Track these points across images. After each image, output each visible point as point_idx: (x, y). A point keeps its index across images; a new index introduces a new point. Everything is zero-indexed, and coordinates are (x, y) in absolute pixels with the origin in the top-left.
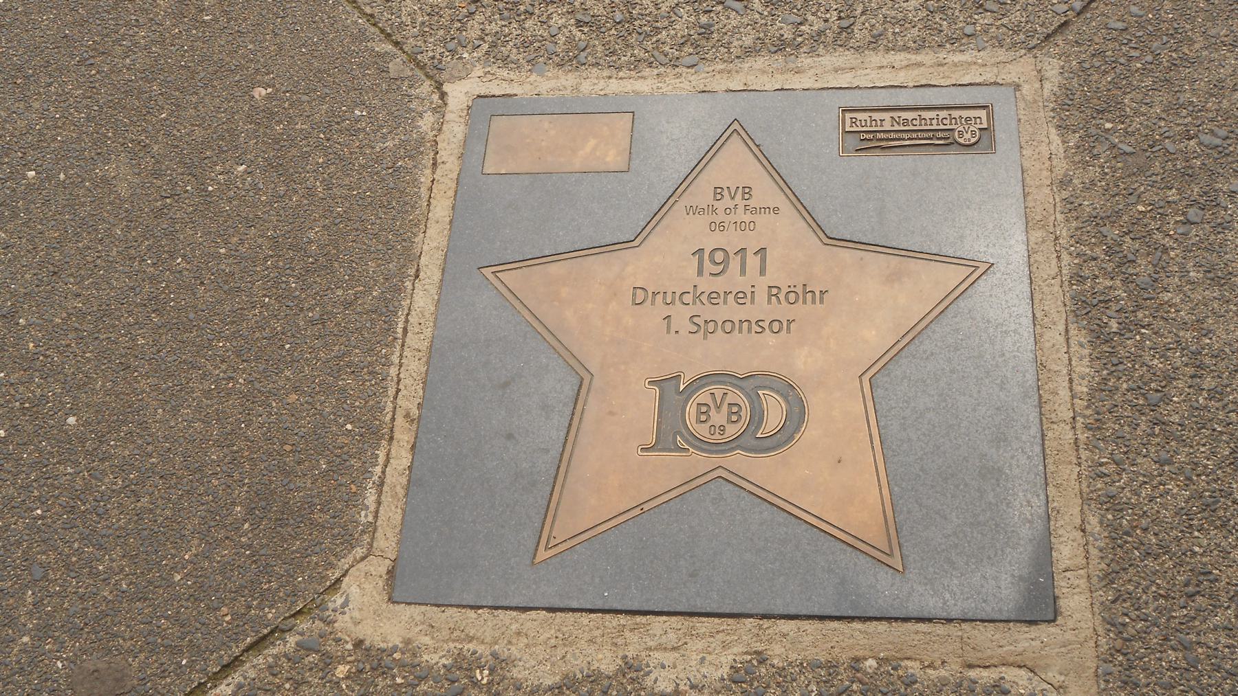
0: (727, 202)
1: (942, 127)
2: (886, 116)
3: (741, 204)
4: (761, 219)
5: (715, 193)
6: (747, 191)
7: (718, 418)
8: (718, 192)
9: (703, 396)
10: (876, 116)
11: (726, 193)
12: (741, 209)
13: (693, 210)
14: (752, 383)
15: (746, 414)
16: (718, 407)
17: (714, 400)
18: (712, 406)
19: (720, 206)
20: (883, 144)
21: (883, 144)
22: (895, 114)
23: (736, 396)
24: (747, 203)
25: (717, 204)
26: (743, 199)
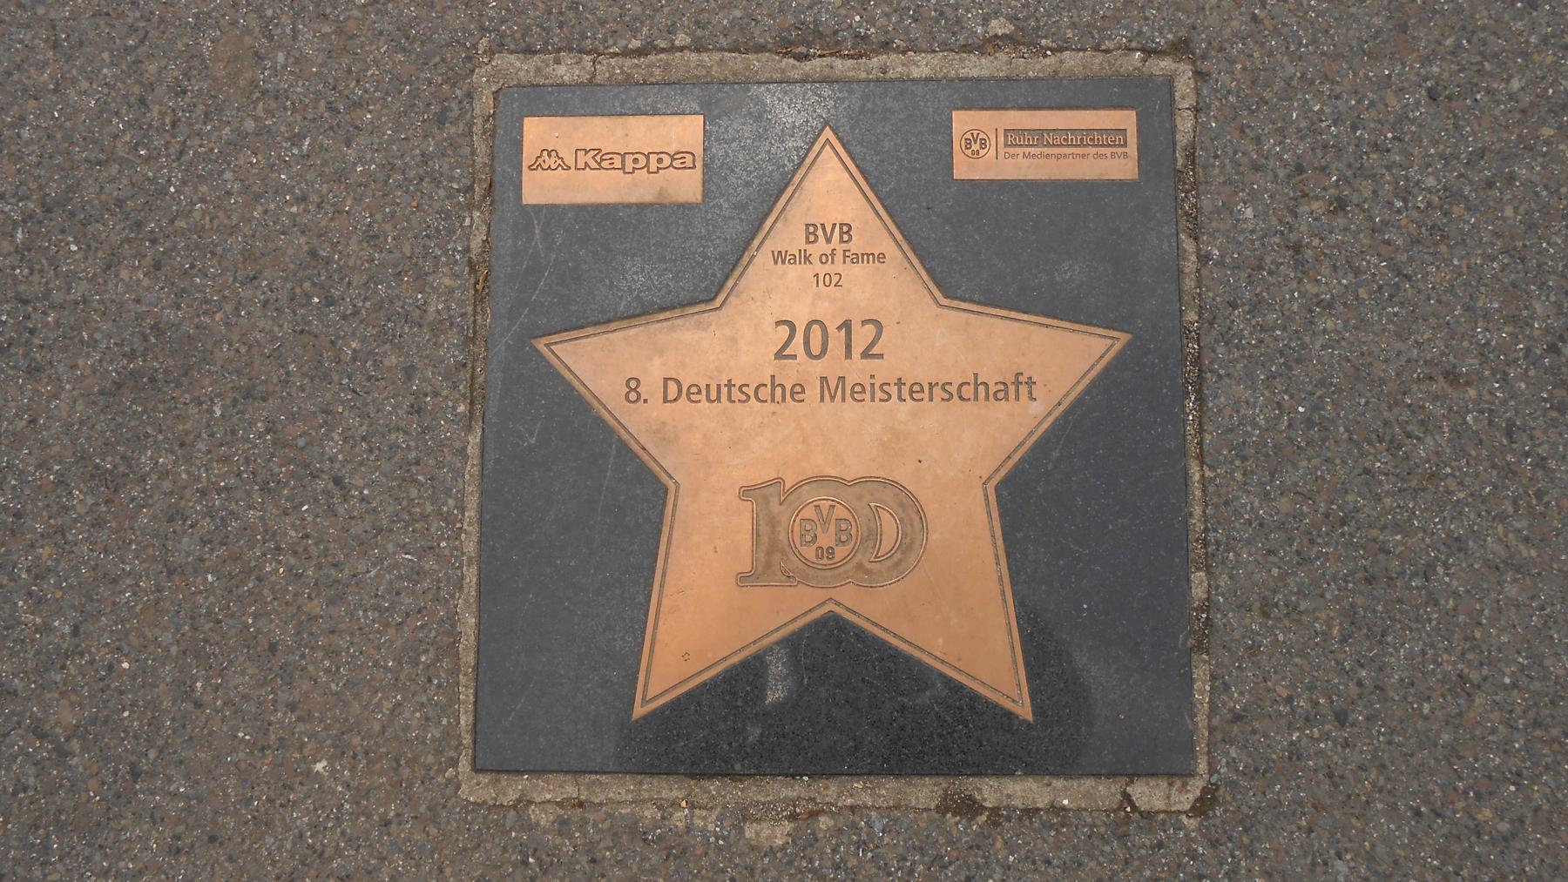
0: (821, 246)
3: (840, 248)
5: (808, 233)
8: (811, 232)
11: (820, 232)
13: (779, 258)
24: (845, 246)
25: (810, 248)
26: (842, 241)
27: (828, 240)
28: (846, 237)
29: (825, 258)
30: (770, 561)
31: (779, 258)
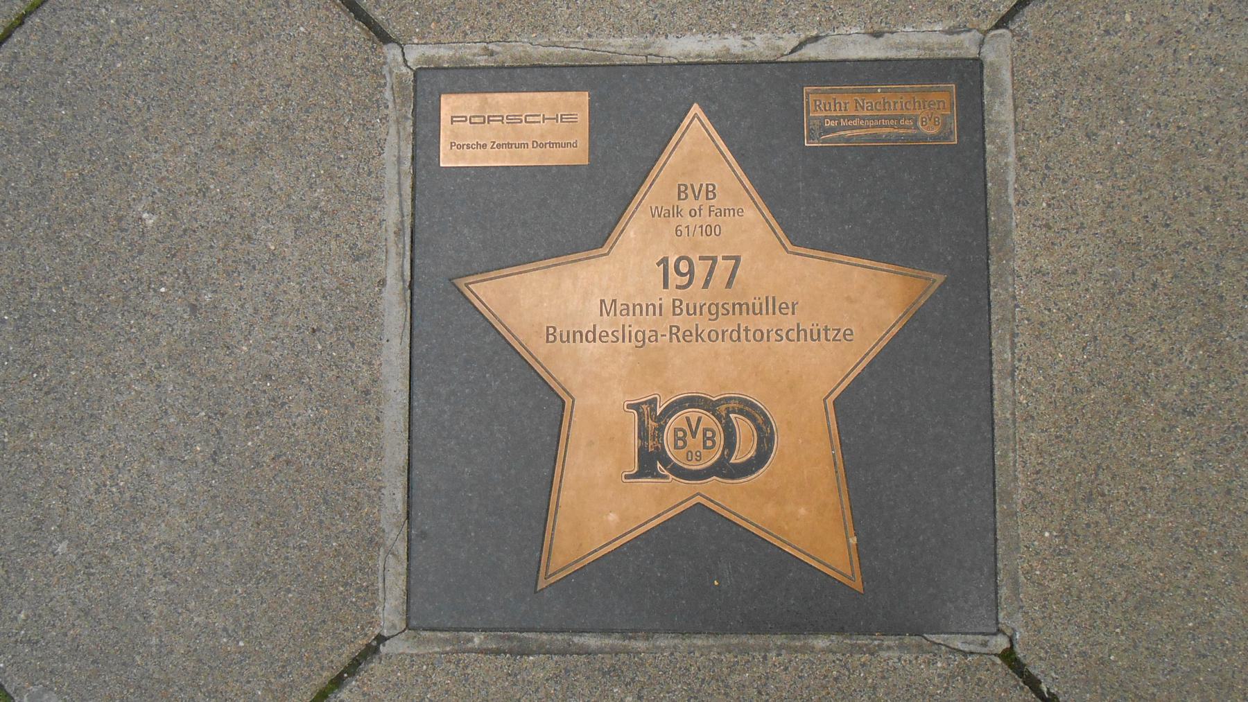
4: (727, 223)
6: (710, 192)
8: (682, 192)
11: (689, 191)
12: (705, 212)
13: (656, 213)
15: (720, 440)
16: (694, 437)
17: (690, 426)
19: (685, 206)
20: (848, 133)
21: (848, 133)
23: (709, 420)
27: (696, 198)
29: (693, 213)
30: (650, 462)
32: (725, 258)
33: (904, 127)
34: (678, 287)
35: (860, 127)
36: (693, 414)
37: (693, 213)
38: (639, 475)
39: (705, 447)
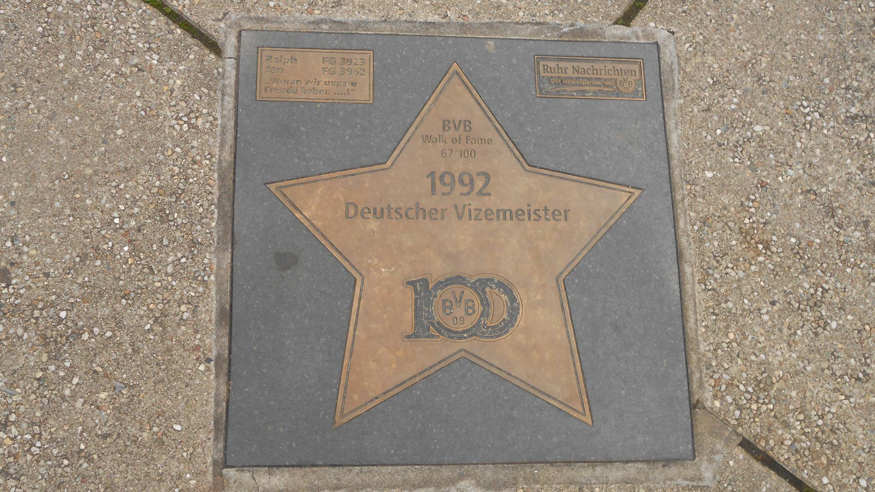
1: (608, 76)
2: (569, 65)
6: (467, 124)
7: (459, 312)
8: (446, 124)
9: (447, 293)
10: (562, 64)
12: (463, 140)
13: (427, 138)
14: (481, 285)
15: (479, 309)
18: (453, 300)
22: (576, 64)
23: (469, 294)
28: (468, 128)
29: (454, 141)
30: (424, 326)
31: (427, 138)
32: (478, 174)
33: (608, 86)
34: (443, 194)
35: (576, 85)
36: (457, 289)
37: (454, 141)
38: (415, 336)
39: (468, 314)
